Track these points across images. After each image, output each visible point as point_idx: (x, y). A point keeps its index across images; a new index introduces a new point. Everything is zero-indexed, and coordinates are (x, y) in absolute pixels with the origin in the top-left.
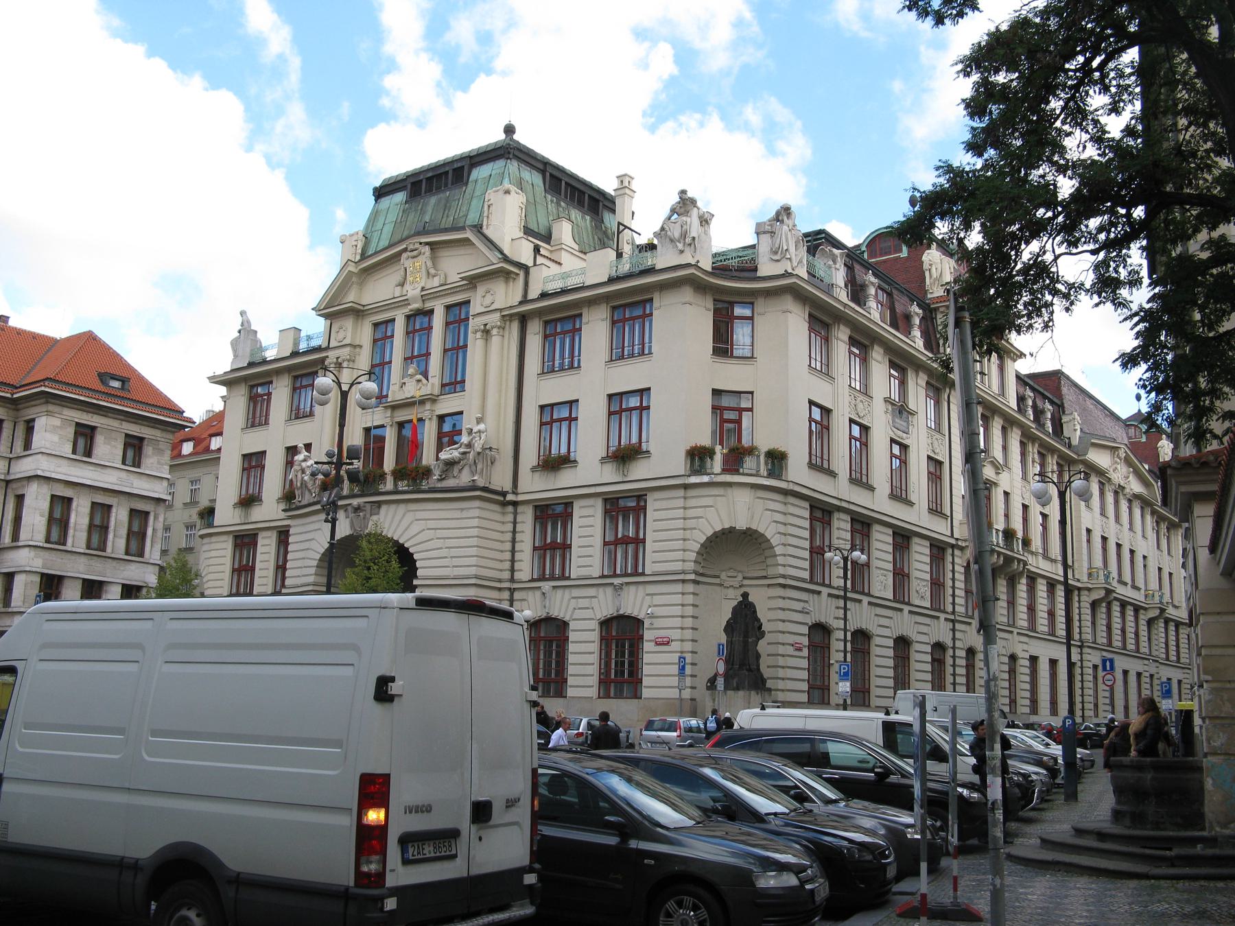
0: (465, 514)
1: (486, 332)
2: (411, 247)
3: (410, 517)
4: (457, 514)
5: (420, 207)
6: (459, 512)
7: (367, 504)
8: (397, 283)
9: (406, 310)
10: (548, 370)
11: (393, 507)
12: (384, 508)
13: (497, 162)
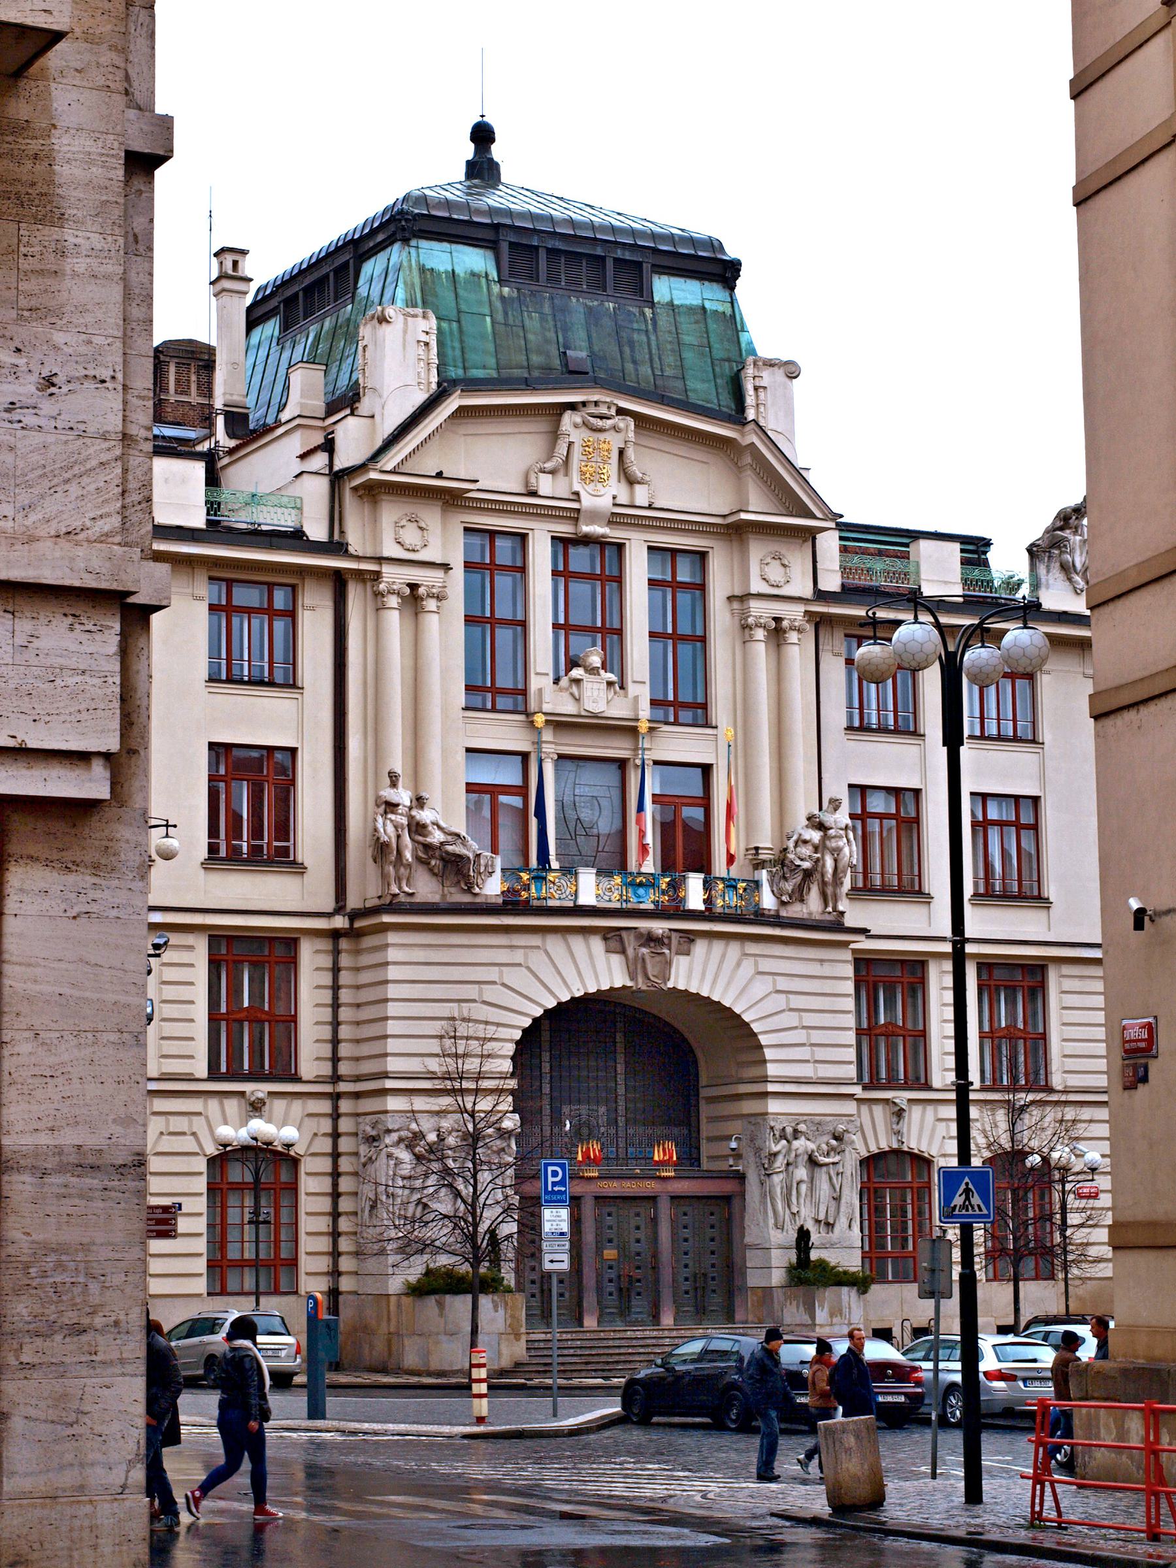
0: (827, 970)
1: (777, 632)
2: (603, 410)
3: (748, 967)
4: (814, 969)
5: (547, 309)
6: (817, 966)
7: (674, 935)
8: (549, 465)
9: (564, 529)
10: (859, 728)
11: (718, 946)
12: (700, 947)
13: (706, 283)
